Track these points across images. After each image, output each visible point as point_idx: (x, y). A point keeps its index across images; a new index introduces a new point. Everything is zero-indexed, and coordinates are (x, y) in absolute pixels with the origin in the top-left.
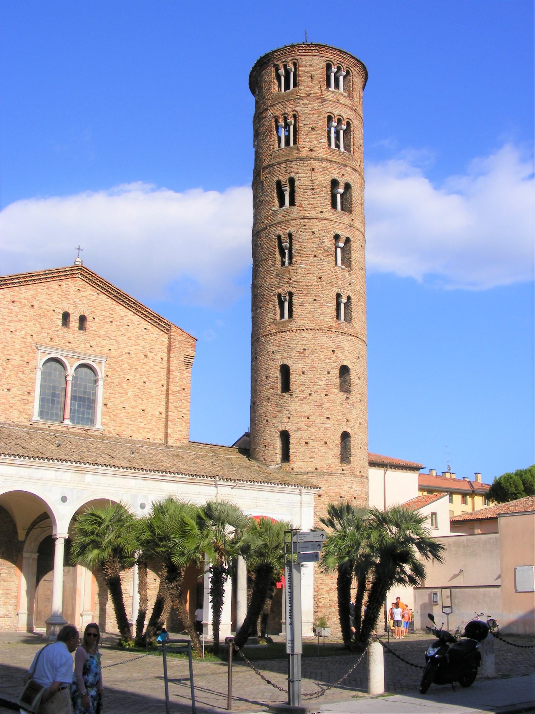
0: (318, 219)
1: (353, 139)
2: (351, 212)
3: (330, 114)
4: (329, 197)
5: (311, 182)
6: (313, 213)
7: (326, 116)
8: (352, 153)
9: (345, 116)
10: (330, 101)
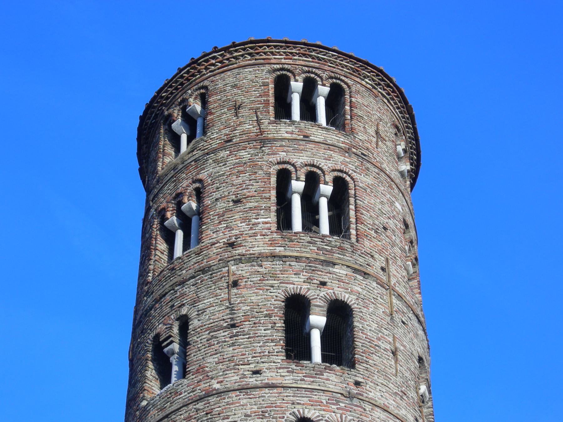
0: (244, 389)
1: (356, 211)
2: (352, 365)
3: (285, 166)
4: (280, 335)
5: (228, 311)
6: (233, 379)
7: (273, 170)
8: (353, 239)
9: (326, 165)
10: (282, 139)
